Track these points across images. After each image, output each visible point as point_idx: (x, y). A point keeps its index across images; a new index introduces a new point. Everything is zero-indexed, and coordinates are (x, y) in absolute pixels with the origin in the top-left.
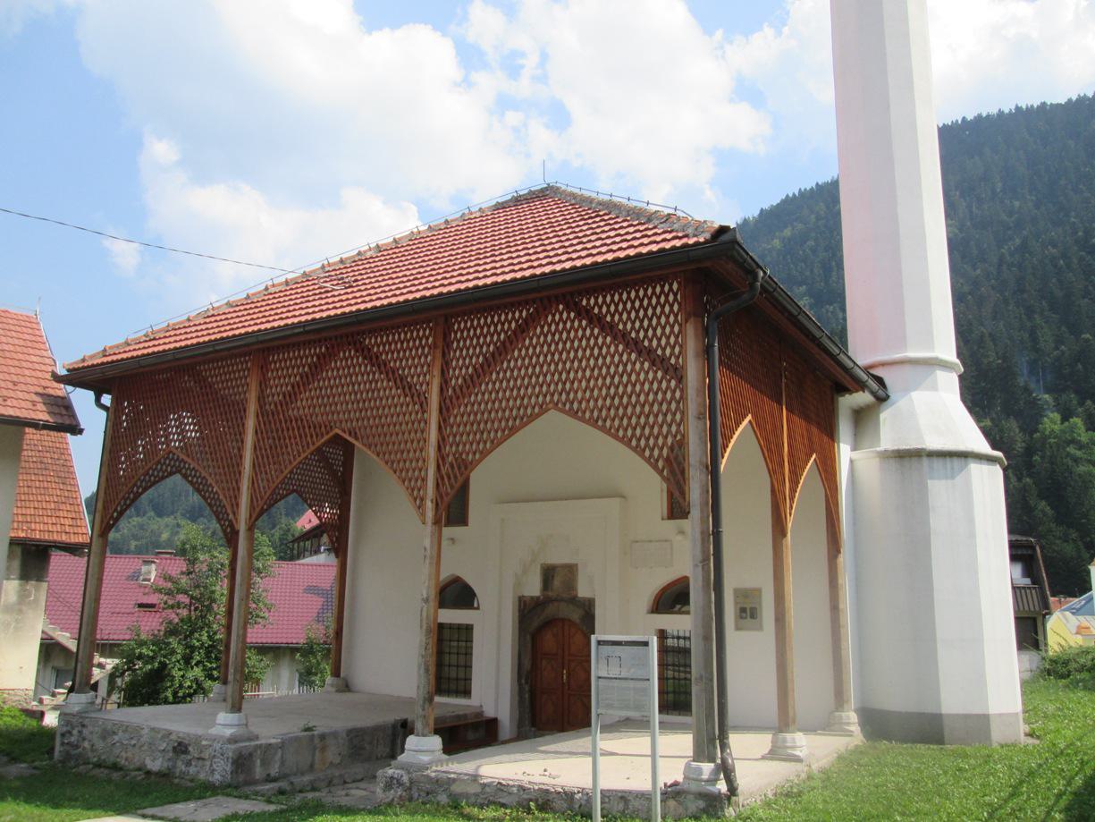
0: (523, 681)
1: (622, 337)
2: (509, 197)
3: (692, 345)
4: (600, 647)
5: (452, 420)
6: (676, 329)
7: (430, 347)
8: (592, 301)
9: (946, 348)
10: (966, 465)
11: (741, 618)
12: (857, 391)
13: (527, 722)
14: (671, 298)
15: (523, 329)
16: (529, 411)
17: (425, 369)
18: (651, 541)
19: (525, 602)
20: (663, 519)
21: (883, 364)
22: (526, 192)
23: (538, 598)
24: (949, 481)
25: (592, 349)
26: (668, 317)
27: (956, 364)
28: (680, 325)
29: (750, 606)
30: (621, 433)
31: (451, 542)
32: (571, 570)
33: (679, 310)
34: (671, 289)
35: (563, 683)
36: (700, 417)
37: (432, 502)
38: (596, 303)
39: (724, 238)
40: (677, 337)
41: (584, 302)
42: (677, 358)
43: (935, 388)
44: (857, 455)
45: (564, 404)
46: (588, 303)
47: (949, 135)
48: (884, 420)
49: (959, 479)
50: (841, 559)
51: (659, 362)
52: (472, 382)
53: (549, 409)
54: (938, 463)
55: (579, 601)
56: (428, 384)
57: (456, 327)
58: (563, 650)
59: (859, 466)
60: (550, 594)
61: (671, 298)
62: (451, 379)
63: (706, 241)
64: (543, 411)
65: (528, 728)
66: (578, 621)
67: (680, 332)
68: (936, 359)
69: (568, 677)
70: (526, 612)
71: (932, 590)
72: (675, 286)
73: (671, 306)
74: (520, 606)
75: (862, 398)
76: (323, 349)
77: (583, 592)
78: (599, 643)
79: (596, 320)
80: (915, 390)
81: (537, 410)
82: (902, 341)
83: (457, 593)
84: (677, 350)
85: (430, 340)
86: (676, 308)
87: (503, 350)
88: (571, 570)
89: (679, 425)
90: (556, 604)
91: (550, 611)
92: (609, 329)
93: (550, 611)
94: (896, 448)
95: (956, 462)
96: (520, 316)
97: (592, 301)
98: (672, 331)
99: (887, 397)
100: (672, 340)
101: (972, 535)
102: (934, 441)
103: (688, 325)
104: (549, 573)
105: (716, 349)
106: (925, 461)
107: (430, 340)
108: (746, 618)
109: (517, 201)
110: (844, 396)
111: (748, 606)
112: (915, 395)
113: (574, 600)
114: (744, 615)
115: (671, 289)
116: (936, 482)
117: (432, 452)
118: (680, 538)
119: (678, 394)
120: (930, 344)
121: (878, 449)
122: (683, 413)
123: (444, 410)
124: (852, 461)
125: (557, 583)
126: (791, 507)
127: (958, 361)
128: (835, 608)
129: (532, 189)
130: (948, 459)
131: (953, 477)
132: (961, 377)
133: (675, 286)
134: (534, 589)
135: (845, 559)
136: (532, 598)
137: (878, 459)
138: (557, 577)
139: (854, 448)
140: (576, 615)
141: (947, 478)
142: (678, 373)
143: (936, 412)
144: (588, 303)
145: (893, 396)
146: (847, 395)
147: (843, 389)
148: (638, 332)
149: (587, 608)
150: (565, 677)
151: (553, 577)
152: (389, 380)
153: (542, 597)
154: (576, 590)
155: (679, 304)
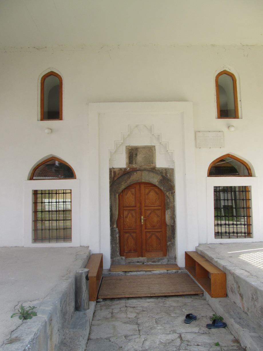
0: (115, 226)
13: (118, 254)
19: (115, 172)
23: (125, 169)
31: (50, 131)
32: (150, 150)
35: (141, 226)
55: (158, 170)
58: (141, 204)
60: (134, 166)
65: (119, 258)
66: (157, 184)
69: (145, 220)
70: (116, 179)
74: (110, 174)
77: (160, 163)
83: (55, 168)
88: (150, 150)
90: (139, 172)
91: (135, 177)
93: (135, 177)
104: (132, 153)
113: (154, 170)
118: (232, 129)
125: (140, 158)
136: (121, 169)
140: (155, 180)
149: (164, 175)
150: (142, 221)
151: (136, 155)
153: (128, 169)
154: (155, 163)
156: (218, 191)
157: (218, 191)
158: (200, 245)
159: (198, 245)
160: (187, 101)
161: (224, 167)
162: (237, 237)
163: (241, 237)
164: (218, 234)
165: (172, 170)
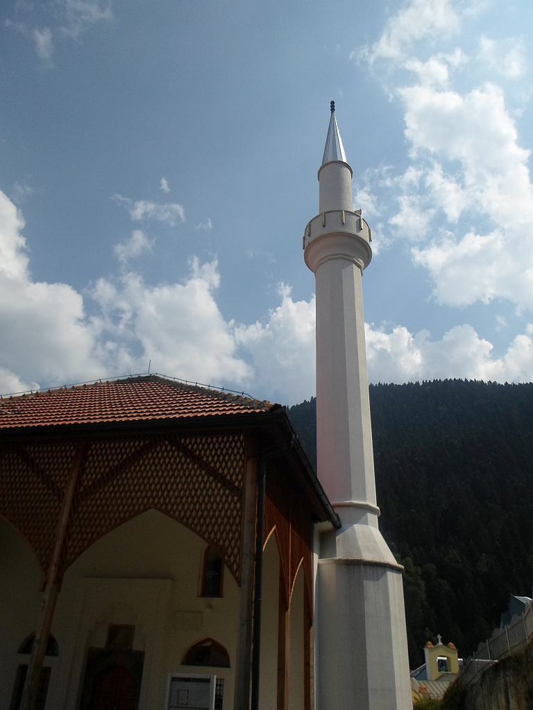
1: (205, 466)
2: (126, 378)
3: (249, 476)
4: (174, 682)
5: (80, 509)
6: (240, 463)
7: (72, 458)
8: (188, 441)
9: (373, 503)
10: (385, 572)
12: (325, 521)
14: (239, 444)
16: (136, 508)
17: (66, 472)
18: (188, 612)
20: (198, 597)
21: (339, 506)
22: (137, 376)
24: (376, 582)
25: (185, 471)
26: (235, 456)
27: (378, 510)
28: (243, 462)
30: (198, 528)
32: (130, 630)
33: (243, 453)
34: (239, 439)
36: (252, 521)
37: (56, 566)
38: (190, 442)
39: (278, 411)
40: (240, 469)
41: (183, 441)
42: (240, 482)
43: (367, 524)
44: (322, 561)
45: (162, 505)
46: (185, 442)
47: (371, 387)
48: (338, 541)
49: (380, 581)
50: (312, 630)
51: (228, 484)
53: (151, 508)
54: (369, 570)
56: (66, 482)
57: (93, 447)
59: (325, 569)
61: (239, 444)
62: (84, 481)
63: (266, 412)
64: (146, 509)
67: (243, 466)
68: (368, 505)
71: (365, 655)
72: (242, 438)
73: (238, 449)
75: (327, 525)
77: (137, 646)
78: (174, 679)
79: (188, 453)
80: (356, 523)
81: (142, 508)
82: (349, 494)
84: (240, 477)
85: (73, 453)
86: (241, 451)
88: (130, 630)
89: (237, 526)
92: (196, 459)
94: (345, 558)
95: (380, 570)
97: (188, 441)
98: (237, 465)
99: (340, 526)
100: (237, 470)
101: (388, 618)
102: (367, 556)
103: (248, 462)
104: (114, 631)
105: (264, 479)
106: (362, 567)
107: (73, 453)
109: (131, 381)
110: (317, 523)
112: (357, 527)
115: (239, 439)
116: (368, 581)
117: (61, 531)
119: (238, 505)
120: (364, 498)
121: (336, 558)
122: (241, 518)
123: (75, 502)
124: (319, 565)
126: (291, 588)
127: (378, 508)
128: (307, 665)
129: (141, 376)
130: (375, 568)
131: (378, 580)
132: (379, 518)
133: (242, 438)
134: (101, 642)
135: (314, 630)
137: (334, 565)
138: (120, 635)
139: (320, 558)
141: (374, 580)
142: (239, 492)
143: (368, 539)
144: (185, 442)
145: (343, 526)
146: (319, 523)
147: (318, 519)
148: (216, 463)
152: (38, 477)
155: (244, 449)
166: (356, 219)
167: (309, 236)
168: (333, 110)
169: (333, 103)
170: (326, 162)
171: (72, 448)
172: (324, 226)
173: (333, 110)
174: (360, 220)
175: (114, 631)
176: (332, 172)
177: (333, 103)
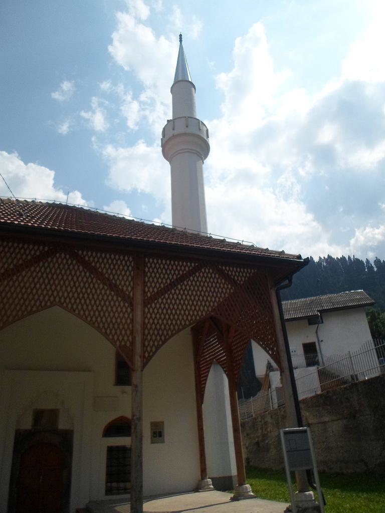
11: (154, 437)
15: (191, 273)
22: (58, 203)
29: (158, 431)
32: (54, 413)
37: (140, 357)
52: (161, 293)
76: (46, 249)
77: (62, 425)
78: (286, 433)
87: (181, 280)
88: (54, 413)
96: (191, 265)
103: (272, 290)
104: (39, 415)
108: (156, 437)
111: (158, 431)
114: (155, 435)
123: (146, 303)
138: (44, 418)
156: (111, 450)
157: (111, 450)
158: (90, 502)
159: (87, 502)
160: (89, 371)
161: (119, 427)
162: (119, 494)
163: (122, 494)
164: (109, 491)
165: (72, 431)
166: (205, 129)
167: (173, 129)
168: (181, 41)
169: (181, 35)
170: (180, 78)
171: (131, 259)
172: (187, 126)
173: (181, 41)
174: (207, 130)
175: (39, 415)
176: (183, 88)
177: (181, 35)
